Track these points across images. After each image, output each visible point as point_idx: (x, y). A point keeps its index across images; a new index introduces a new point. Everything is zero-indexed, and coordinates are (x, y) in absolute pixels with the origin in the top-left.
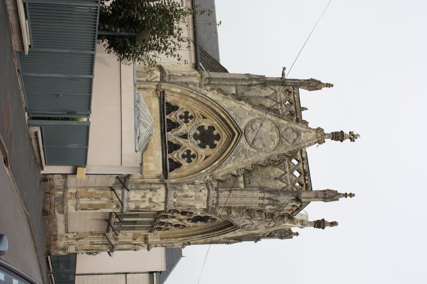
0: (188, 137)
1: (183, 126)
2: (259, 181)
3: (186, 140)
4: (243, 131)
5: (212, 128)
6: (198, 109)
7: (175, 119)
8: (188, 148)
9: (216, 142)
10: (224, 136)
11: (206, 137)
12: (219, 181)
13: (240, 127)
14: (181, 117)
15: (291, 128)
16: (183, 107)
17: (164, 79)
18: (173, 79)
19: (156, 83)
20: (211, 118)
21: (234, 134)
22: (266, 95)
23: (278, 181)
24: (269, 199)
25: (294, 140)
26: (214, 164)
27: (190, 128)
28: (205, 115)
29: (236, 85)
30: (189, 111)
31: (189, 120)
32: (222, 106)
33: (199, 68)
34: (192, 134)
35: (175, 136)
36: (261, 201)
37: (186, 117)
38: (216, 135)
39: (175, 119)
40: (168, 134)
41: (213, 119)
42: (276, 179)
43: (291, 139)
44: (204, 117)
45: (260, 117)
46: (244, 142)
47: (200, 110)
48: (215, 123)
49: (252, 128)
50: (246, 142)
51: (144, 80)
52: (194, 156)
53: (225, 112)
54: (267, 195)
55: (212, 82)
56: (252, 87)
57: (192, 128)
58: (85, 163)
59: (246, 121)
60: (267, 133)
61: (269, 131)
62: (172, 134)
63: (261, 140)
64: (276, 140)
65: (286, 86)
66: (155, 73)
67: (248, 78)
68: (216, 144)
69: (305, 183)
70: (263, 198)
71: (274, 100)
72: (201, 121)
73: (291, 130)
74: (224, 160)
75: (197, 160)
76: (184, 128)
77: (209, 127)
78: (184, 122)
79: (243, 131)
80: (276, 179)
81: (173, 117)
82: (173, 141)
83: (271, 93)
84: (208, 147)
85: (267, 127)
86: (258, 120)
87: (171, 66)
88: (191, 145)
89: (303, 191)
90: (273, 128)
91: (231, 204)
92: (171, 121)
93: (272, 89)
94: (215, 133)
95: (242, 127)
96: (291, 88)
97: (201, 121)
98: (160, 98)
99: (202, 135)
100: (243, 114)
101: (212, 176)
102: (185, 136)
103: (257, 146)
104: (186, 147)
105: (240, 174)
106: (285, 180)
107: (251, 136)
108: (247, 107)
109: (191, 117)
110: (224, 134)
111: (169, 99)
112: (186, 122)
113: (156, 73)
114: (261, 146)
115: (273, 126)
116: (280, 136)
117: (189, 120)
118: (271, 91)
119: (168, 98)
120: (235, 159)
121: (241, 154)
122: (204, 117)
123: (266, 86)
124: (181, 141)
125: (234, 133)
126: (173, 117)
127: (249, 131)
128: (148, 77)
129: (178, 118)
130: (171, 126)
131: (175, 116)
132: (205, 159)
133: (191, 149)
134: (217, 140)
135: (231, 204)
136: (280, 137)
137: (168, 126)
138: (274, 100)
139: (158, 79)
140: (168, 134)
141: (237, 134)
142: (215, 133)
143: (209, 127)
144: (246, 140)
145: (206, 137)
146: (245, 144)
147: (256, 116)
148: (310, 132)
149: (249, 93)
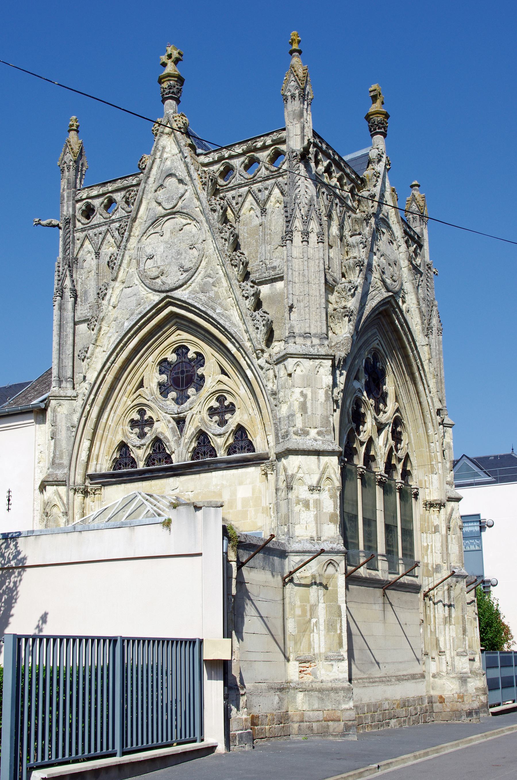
0: (182, 415)
1: (159, 430)
2: (268, 247)
3: (187, 420)
4: (164, 295)
5: (164, 365)
6: (124, 398)
7: (145, 447)
8: (205, 414)
9: (191, 355)
10: (179, 337)
11: (182, 377)
12: (269, 339)
13: (155, 303)
14: (142, 435)
15: (156, 191)
16: (120, 432)
17: (60, 477)
18: (61, 458)
19: (71, 493)
20: (141, 370)
21: (172, 315)
22: (94, 257)
23: (267, 207)
24: (306, 223)
25: (181, 181)
26: (233, 352)
27: (162, 414)
28: (135, 382)
29: (75, 324)
30: (128, 420)
31: (146, 417)
32: (113, 346)
33: (43, 406)
34: (174, 407)
35: (179, 445)
36: (313, 238)
37: (142, 424)
38: (178, 355)
39: (145, 447)
40: (176, 460)
41: (144, 366)
42: (264, 211)
43: (177, 188)
44: (141, 385)
45: (134, 262)
46: (187, 291)
47: (127, 394)
48: (151, 359)
49: (158, 277)
50: (185, 286)
51: (64, 520)
52: (221, 399)
53: (125, 340)
54: (298, 224)
55: (69, 374)
56: (78, 288)
57: (161, 408)
58: (192, 642)
59: (143, 291)
60: (166, 242)
61: (162, 238)
62: (176, 452)
63: (181, 254)
64: (182, 220)
65: (74, 216)
66: (49, 498)
67: (58, 298)
68: (195, 353)
69: (270, 146)
70: (306, 234)
71: (104, 239)
72: (147, 392)
73: (160, 192)
74: (224, 331)
75: (228, 392)
76: (164, 427)
77: (161, 372)
78: (151, 427)
79: (164, 295)
80: (264, 211)
81: (140, 455)
82: (191, 449)
83: (90, 246)
84: (200, 371)
85: (154, 244)
86: (142, 265)
87: (41, 464)
88: (198, 408)
89: (288, 147)
90: (156, 230)
91: (320, 304)
92: (149, 457)
93: (82, 245)
94: (172, 357)
95: (156, 298)
96: (78, 205)
97: (147, 392)
98: (104, 485)
99: (179, 386)
100: (129, 300)
101: (259, 353)
102: (180, 422)
103: (194, 261)
104: (202, 419)
105: (252, 291)
106: (267, 192)
107: (173, 278)
108: (115, 292)
109: (142, 412)
110: (173, 338)
111: (103, 464)
112: (150, 422)
113: (48, 495)
114: (195, 252)
115: (152, 231)
116: (172, 213)
117: (146, 417)
118: (87, 247)
119: (104, 467)
120: (222, 306)
121: (212, 294)
122: (141, 385)
123: (77, 259)
124: (190, 430)
125: (171, 315)
126: (140, 455)
127: (164, 283)
128: (58, 512)
129: (143, 441)
130: (160, 456)
131: (139, 447)
132: (226, 374)
133: (207, 407)
134: (187, 353)
135: (320, 304)
136: (174, 213)
137: (160, 465)
138: (104, 239)
139: (62, 490)
140: (176, 460)
141: (171, 308)
142: (172, 357)
143: (161, 372)
144: (181, 286)
145: (182, 377)
146: (190, 289)
147: (133, 269)
148: (164, 148)
149: (92, 294)
